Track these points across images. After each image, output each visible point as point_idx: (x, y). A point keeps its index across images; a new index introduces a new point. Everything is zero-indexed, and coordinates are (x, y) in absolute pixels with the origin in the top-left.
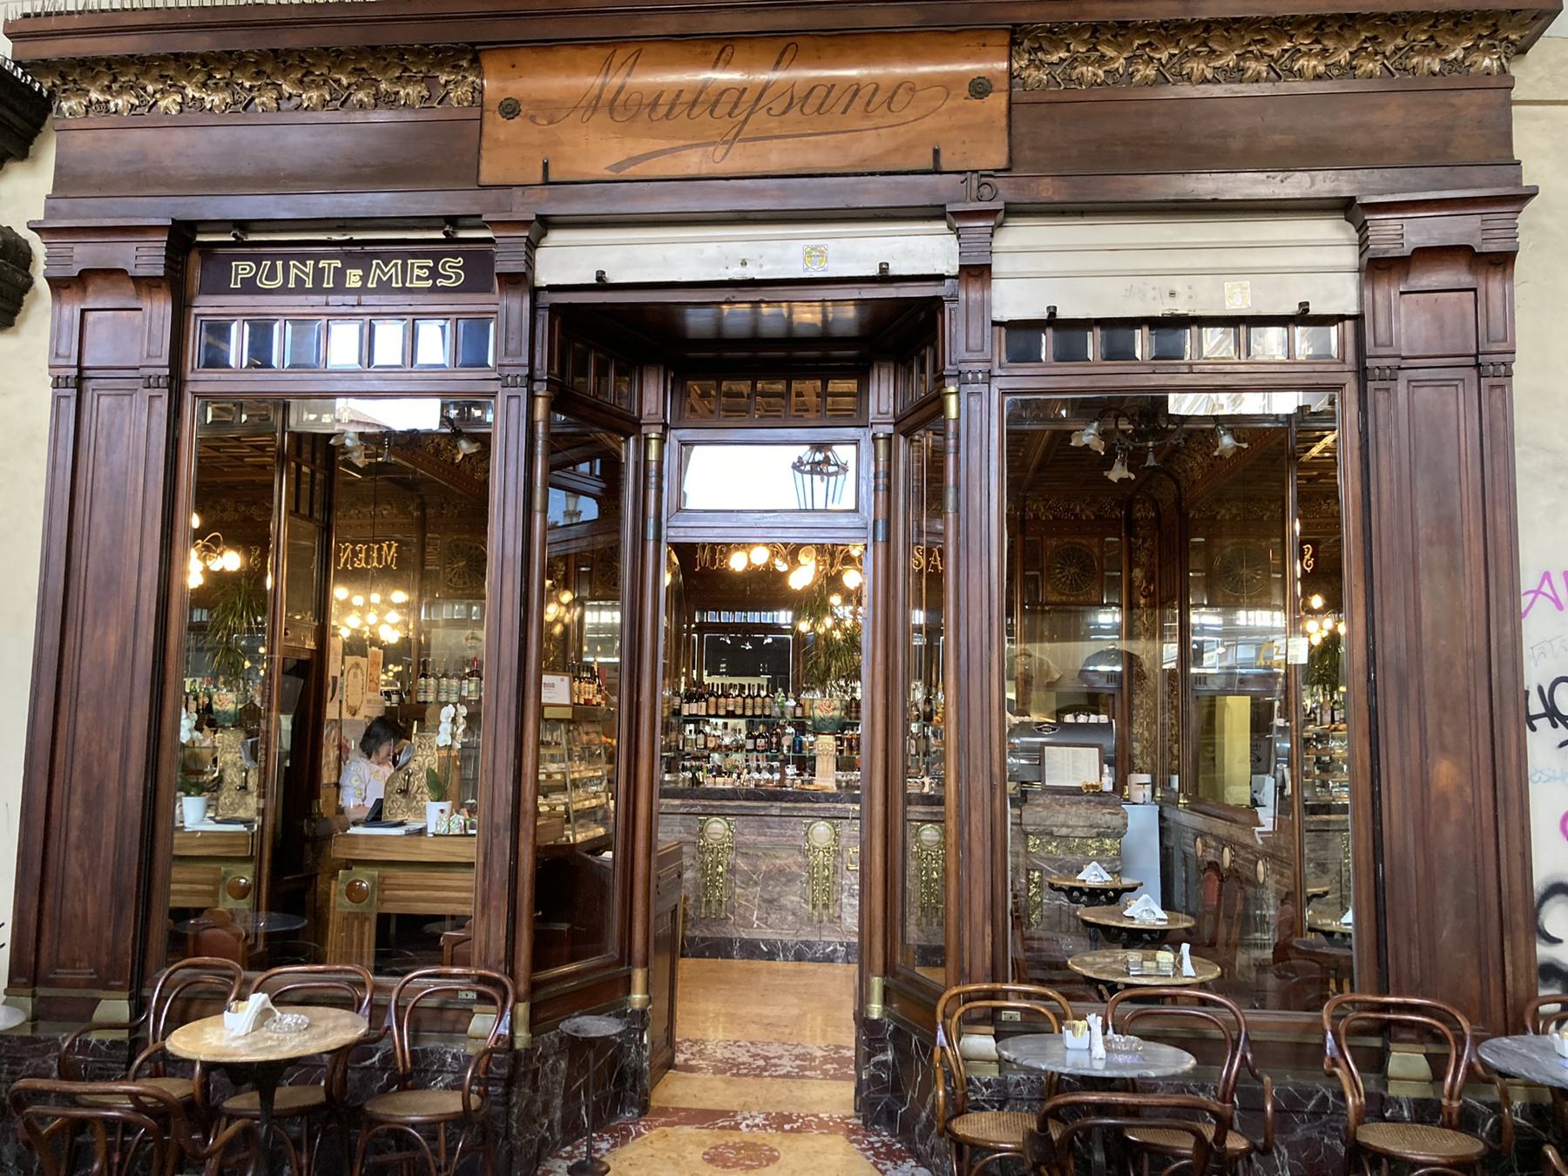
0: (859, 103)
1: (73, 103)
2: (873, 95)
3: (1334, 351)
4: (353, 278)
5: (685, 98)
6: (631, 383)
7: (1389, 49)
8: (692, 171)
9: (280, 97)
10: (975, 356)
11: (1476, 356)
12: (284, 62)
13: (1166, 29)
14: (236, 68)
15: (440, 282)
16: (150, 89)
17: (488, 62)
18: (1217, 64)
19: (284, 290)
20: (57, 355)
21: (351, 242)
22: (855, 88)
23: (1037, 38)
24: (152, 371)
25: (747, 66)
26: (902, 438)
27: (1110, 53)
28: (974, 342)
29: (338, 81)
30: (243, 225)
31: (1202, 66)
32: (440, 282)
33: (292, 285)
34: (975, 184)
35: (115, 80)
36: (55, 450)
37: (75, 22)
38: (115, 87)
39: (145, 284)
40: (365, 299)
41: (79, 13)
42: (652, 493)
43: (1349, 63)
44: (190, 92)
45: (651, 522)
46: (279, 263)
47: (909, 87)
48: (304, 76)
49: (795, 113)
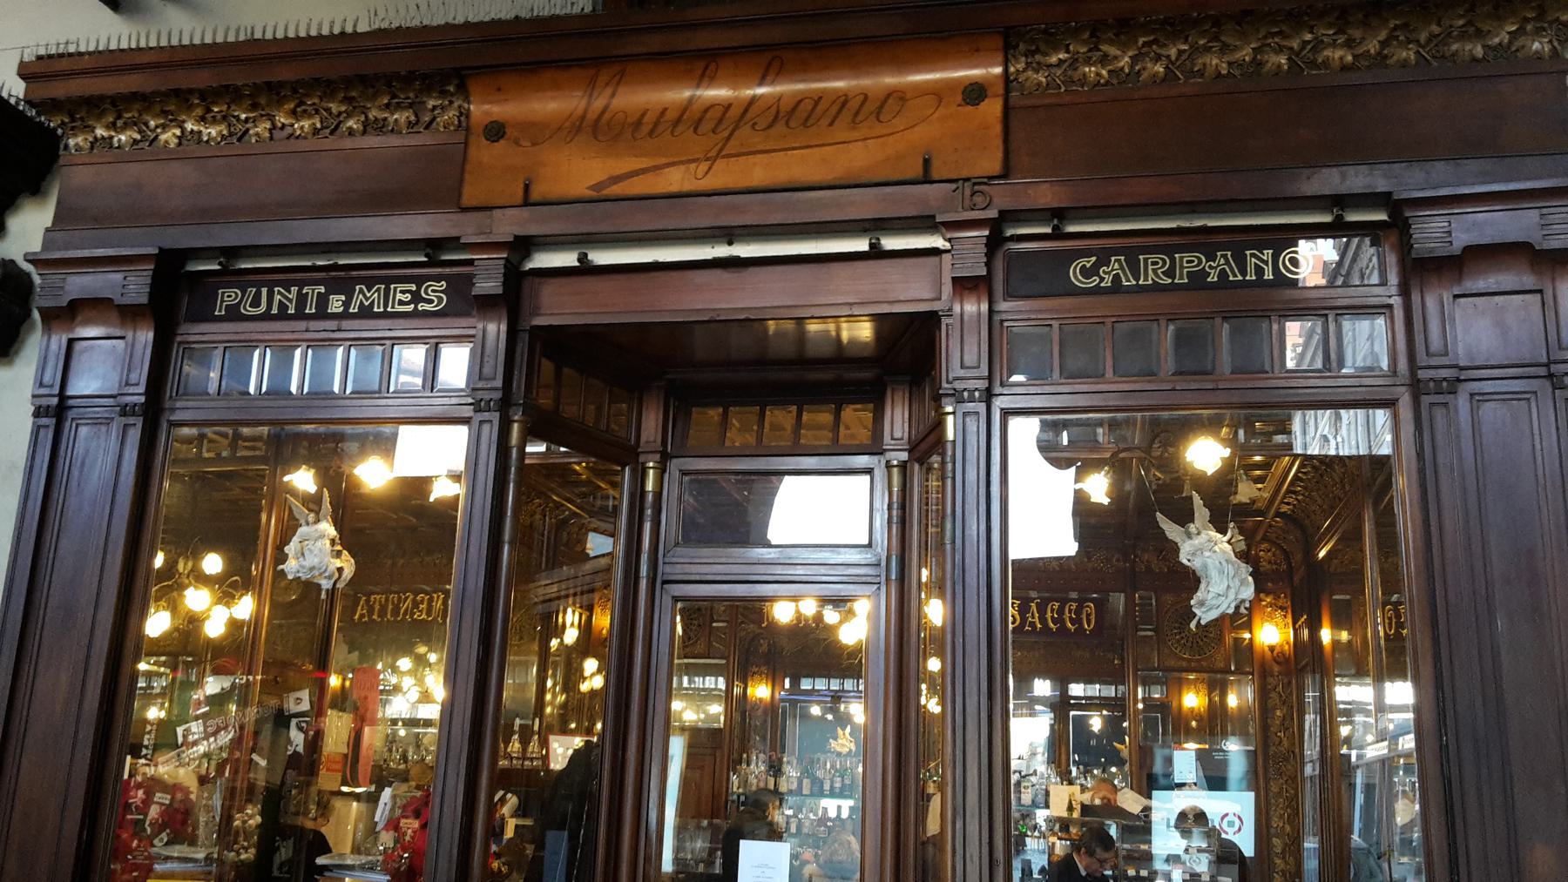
0: (846, 115)
1: (80, 139)
2: (862, 105)
3: (1385, 365)
4: (336, 304)
5: (671, 115)
6: (630, 409)
7: (1423, 37)
8: (674, 188)
9: (274, 127)
10: (969, 373)
11: (1547, 365)
12: (278, 94)
13: (1172, 25)
14: (233, 101)
15: (422, 307)
16: (152, 124)
17: (473, 87)
18: (1231, 58)
19: (266, 317)
20: (41, 385)
21: (335, 267)
22: (843, 100)
23: (1033, 41)
24: (129, 399)
25: (734, 80)
26: (917, 466)
27: (1113, 51)
28: (970, 359)
29: (328, 110)
30: (232, 253)
31: (1215, 61)
32: (422, 307)
33: (275, 311)
34: (968, 192)
35: (119, 117)
36: (29, 479)
37: (85, 63)
38: (120, 123)
39: (128, 314)
40: (346, 324)
41: (90, 53)
42: (647, 526)
43: (1379, 54)
44: (189, 126)
45: (644, 558)
46: (264, 291)
47: (899, 97)
48: (298, 105)
49: (780, 128)
